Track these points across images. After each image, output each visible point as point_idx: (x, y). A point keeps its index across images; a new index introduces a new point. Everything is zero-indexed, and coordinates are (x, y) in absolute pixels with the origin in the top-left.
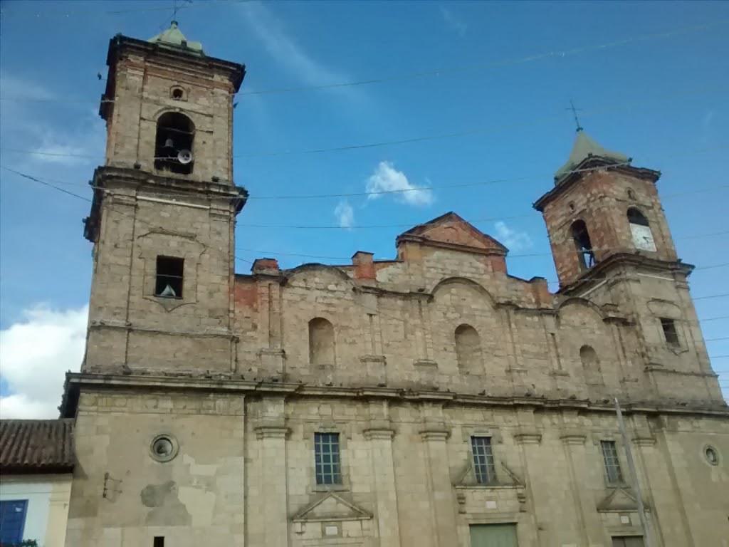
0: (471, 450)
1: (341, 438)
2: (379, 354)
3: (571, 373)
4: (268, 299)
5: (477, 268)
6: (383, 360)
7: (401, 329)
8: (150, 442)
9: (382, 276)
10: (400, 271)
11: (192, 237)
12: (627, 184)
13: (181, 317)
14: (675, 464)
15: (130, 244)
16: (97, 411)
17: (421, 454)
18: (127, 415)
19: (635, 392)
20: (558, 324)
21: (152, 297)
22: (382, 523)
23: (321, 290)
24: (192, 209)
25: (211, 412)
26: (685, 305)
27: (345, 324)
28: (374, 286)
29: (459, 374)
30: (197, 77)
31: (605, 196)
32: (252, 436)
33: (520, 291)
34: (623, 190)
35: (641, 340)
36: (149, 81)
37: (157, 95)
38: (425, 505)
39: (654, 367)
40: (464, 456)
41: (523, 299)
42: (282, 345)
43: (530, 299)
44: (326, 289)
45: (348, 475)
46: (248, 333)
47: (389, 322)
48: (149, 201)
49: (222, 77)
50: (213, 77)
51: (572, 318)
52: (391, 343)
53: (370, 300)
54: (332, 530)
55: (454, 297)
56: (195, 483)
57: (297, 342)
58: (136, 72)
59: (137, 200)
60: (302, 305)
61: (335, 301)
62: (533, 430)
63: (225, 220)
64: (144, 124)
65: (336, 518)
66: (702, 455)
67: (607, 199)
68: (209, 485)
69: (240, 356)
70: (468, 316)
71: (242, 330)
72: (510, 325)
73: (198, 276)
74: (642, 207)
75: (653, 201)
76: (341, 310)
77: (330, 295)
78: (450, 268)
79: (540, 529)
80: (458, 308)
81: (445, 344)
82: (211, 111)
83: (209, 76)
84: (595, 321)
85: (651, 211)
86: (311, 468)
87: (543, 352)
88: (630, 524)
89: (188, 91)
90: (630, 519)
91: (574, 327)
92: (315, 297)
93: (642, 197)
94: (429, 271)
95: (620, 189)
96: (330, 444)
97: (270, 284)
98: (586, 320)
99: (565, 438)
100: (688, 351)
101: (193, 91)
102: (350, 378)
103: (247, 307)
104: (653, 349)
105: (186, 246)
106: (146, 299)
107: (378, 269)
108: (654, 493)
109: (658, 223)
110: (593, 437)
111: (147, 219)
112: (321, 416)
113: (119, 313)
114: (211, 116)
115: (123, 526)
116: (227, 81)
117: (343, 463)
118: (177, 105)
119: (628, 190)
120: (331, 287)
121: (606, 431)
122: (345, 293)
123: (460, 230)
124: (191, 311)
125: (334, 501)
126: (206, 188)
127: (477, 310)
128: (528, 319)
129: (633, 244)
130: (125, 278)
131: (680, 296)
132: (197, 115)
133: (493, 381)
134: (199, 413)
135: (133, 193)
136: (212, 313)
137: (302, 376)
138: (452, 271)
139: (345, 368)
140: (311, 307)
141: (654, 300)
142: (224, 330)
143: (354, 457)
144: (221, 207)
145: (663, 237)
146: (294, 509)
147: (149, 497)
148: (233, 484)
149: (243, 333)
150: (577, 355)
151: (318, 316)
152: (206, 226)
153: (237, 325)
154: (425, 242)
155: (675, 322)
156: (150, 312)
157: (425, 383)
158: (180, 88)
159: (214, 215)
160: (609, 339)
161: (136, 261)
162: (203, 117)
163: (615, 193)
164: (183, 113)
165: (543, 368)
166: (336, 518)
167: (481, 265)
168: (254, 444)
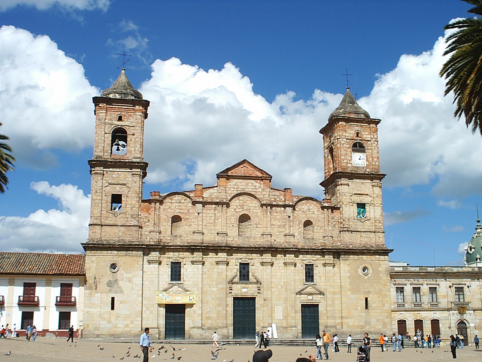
0: (239, 268)
3: (296, 234)
4: (154, 209)
5: (255, 186)
7: (213, 218)
8: (109, 265)
9: (206, 194)
10: (215, 191)
11: (124, 185)
23: (178, 203)
27: (187, 217)
28: (201, 200)
29: (238, 236)
31: (340, 138)
33: (277, 195)
34: (354, 132)
35: (342, 215)
36: (108, 114)
37: (111, 120)
39: (344, 229)
40: (235, 271)
41: (278, 199)
43: (282, 199)
46: (146, 223)
47: (208, 215)
51: (303, 207)
52: (207, 224)
53: (199, 206)
55: (240, 201)
56: (125, 280)
57: (166, 226)
59: (103, 171)
60: (169, 210)
61: (184, 208)
62: (269, 260)
63: (138, 176)
64: (106, 136)
66: (360, 271)
70: (246, 210)
71: (144, 222)
73: (127, 201)
74: (363, 141)
75: (372, 136)
77: (182, 204)
78: (241, 187)
80: (242, 206)
81: (233, 224)
82: (134, 124)
84: (316, 208)
85: (369, 143)
89: (125, 116)
90: (313, 297)
93: (366, 135)
94: (230, 190)
95: (352, 132)
101: (127, 115)
103: (146, 212)
104: (347, 220)
111: (108, 179)
115: (101, 293)
118: (120, 123)
123: (249, 167)
124: (124, 216)
125: (177, 287)
127: (252, 206)
128: (279, 209)
129: (352, 164)
130: (100, 205)
132: (128, 127)
133: (254, 239)
136: (132, 216)
137: (167, 240)
138: (242, 189)
139: (185, 236)
140: (173, 211)
141: (355, 194)
142: (136, 223)
147: (110, 284)
148: (138, 280)
149: (144, 223)
153: (142, 220)
154: (229, 178)
155: (366, 205)
156: (110, 217)
158: (121, 115)
159: (133, 174)
160: (322, 216)
161: (104, 197)
163: (347, 135)
164: (122, 127)
165: (281, 232)
167: (258, 184)
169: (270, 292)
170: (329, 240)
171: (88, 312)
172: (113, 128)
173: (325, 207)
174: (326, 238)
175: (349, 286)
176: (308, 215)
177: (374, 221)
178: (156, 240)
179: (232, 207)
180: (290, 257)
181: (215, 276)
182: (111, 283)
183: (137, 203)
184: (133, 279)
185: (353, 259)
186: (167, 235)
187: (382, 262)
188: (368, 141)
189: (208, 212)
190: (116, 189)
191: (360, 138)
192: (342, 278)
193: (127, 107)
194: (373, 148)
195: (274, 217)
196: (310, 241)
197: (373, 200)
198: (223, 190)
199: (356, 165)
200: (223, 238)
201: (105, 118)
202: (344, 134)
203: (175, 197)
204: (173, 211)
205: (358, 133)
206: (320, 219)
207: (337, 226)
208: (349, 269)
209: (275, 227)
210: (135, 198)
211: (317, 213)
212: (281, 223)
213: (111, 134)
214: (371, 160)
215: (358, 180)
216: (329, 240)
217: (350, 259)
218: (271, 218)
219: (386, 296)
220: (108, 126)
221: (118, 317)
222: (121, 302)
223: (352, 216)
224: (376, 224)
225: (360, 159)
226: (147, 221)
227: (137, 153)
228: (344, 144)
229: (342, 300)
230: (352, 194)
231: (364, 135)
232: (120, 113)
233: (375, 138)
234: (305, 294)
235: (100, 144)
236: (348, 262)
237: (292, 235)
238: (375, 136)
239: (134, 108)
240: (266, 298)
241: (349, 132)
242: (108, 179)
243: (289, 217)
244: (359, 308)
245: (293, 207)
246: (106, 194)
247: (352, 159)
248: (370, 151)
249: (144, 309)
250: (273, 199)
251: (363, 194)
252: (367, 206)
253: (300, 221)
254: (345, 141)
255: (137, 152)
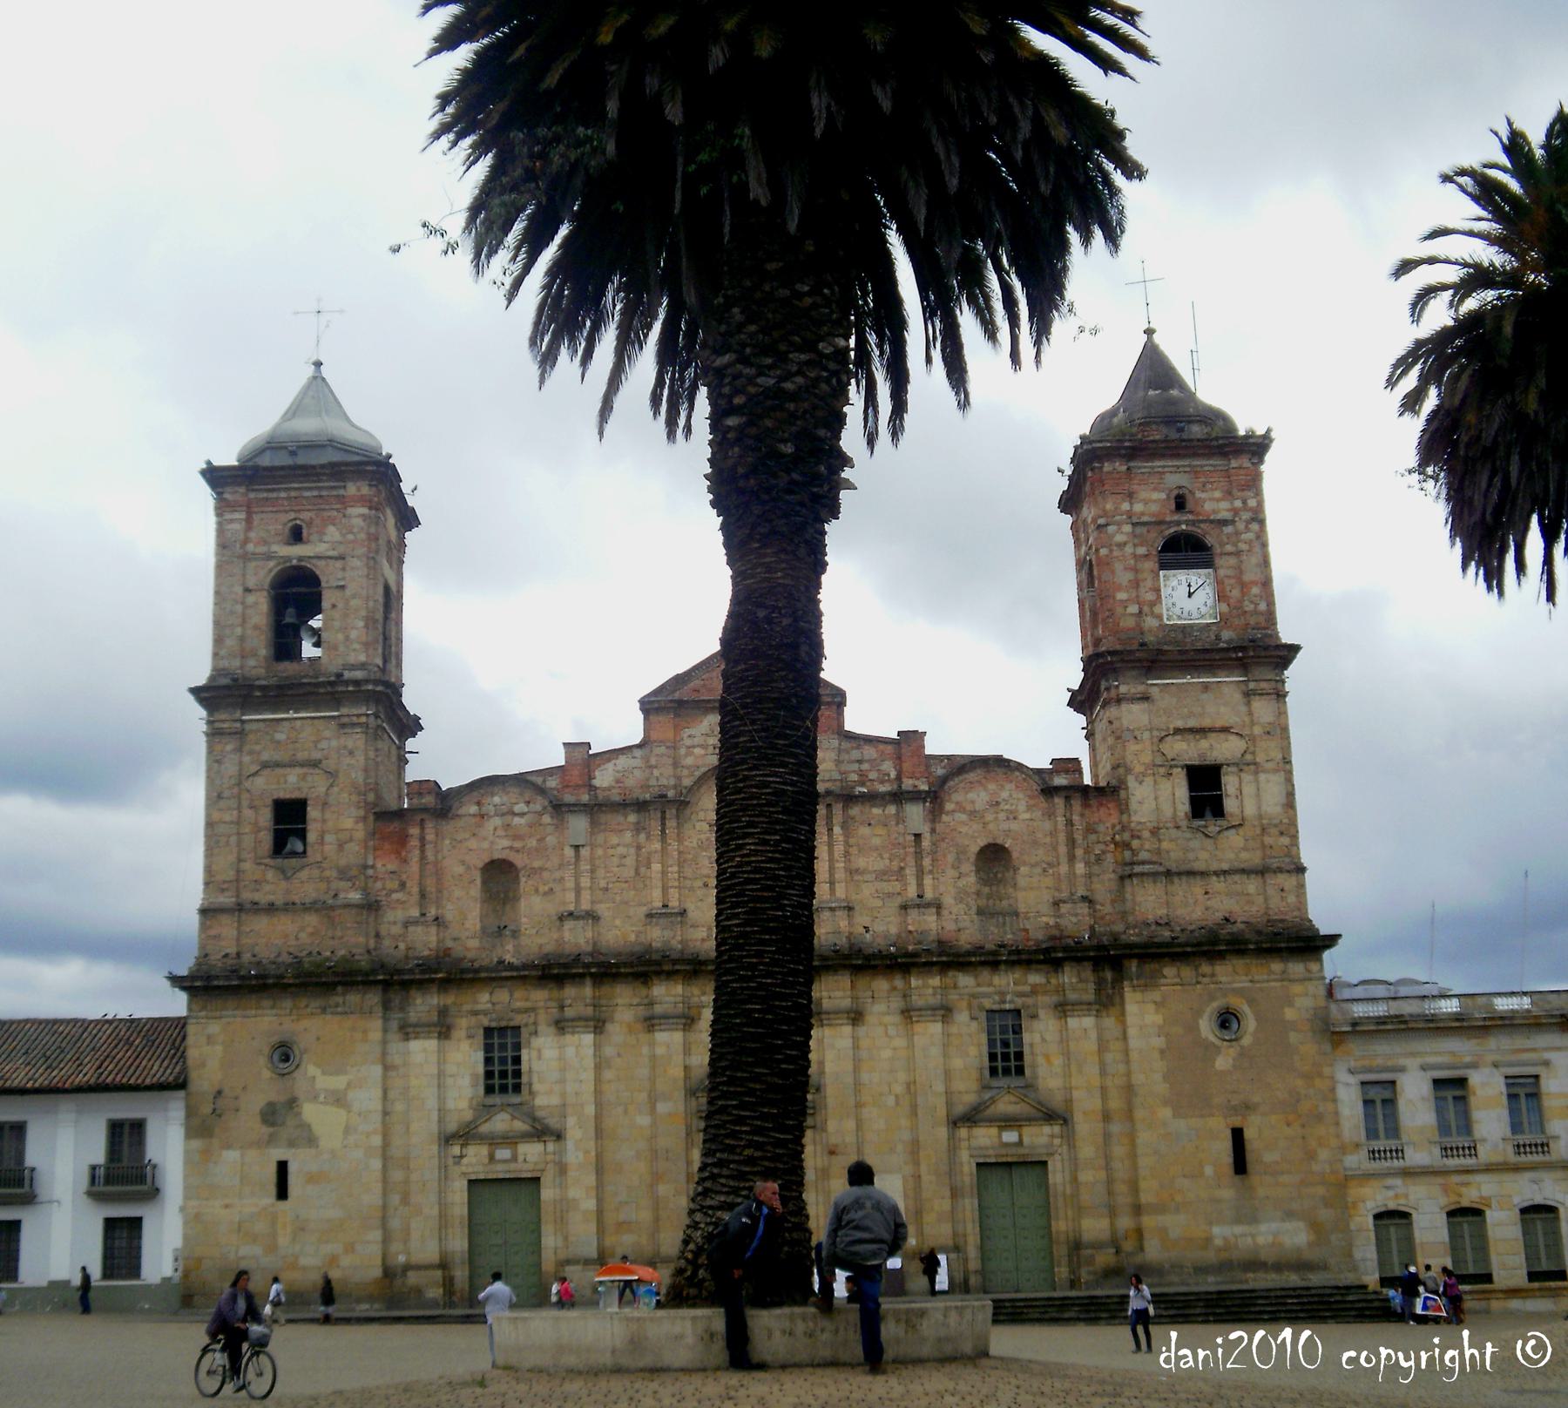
1: (523, 1030)
2: (585, 905)
3: (948, 900)
6: (592, 916)
9: (604, 778)
10: (638, 762)
11: (315, 764)
12: (1175, 480)
13: (306, 885)
14: (1135, 1042)
15: (235, 790)
16: (207, 1018)
17: (645, 1050)
18: (239, 1019)
19: (1076, 923)
20: (935, 814)
21: (267, 861)
22: (570, 1144)
24: (316, 721)
25: (339, 1009)
26: (1257, 730)
27: (537, 864)
28: (585, 798)
30: (321, 496)
31: (1107, 525)
32: (394, 1036)
33: (868, 761)
34: (1163, 496)
35: (1125, 817)
36: (255, 523)
37: (265, 542)
38: (644, 1120)
39: (1138, 869)
41: (873, 775)
42: (437, 909)
44: (515, 814)
45: (530, 1084)
46: (395, 896)
47: (611, 852)
48: (258, 720)
49: (358, 484)
50: (345, 487)
51: (971, 796)
53: (578, 825)
54: (503, 1153)
56: (322, 1098)
58: (237, 516)
59: (243, 722)
60: (473, 844)
64: (251, 599)
65: (510, 1140)
66: (1207, 1027)
67: (1111, 529)
68: (339, 1099)
69: (383, 931)
72: (830, 830)
74: (1202, 525)
75: (1238, 504)
76: (533, 843)
77: (517, 820)
79: (832, 1153)
82: (341, 549)
83: (340, 487)
84: (1021, 796)
85: (1229, 529)
86: (474, 1076)
87: (896, 868)
88: (1020, 1143)
89: (310, 524)
91: (973, 814)
92: (492, 828)
93: (1212, 502)
94: (687, 755)
95: (1155, 496)
96: (509, 1040)
97: (422, 820)
98: (1005, 794)
99: (908, 1014)
100: (1240, 825)
101: (317, 521)
102: (541, 946)
103: (393, 856)
104: (1146, 834)
105: (309, 778)
106: (260, 864)
107: (599, 765)
108: (1076, 1094)
109: (1238, 553)
110: (970, 1007)
111: (257, 748)
112: (493, 1004)
113: (227, 889)
114: (342, 558)
116: (365, 490)
117: (524, 1067)
119: (1175, 492)
120: (517, 808)
121: (1002, 994)
122: (540, 814)
124: (316, 873)
126: (329, 689)
128: (876, 811)
129: (1160, 617)
130: (233, 839)
131: (1250, 714)
132: (322, 563)
134: (324, 1010)
135: (237, 715)
136: (343, 874)
137: (467, 949)
139: (534, 931)
140: (486, 845)
141: (1178, 731)
143: (539, 1058)
144: (355, 711)
145: (1244, 586)
146: (452, 1127)
147: (271, 1115)
148: (367, 1098)
150: (968, 867)
151: (496, 856)
152: (334, 743)
153: (379, 885)
155: (1224, 769)
157: (659, 945)
160: (1048, 825)
162: (331, 562)
163: (1138, 507)
164: (303, 564)
165: (890, 895)
166: (510, 1140)
168: (396, 1046)
169: (850, 1124)
170: (1076, 915)
171: (197, 1216)
172: (270, 571)
173: (1057, 789)
174: (1064, 908)
175: (1162, 1088)
176: (991, 826)
177: (1258, 831)
178: (426, 953)
179: (701, 815)
180: (926, 986)
181: (644, 1072)
182: (274, 1113)
183: (361, 826)
184: (351, 1095)
185: (1177, 980)
186: (467, 934)
187: (1297, 989)
188: (1224, 522)
189: (614, 840)
190: (286, 782)
191: (1191, 517)
192: (1134, 1056)
193: (315, 493)
194: (1242, 546)
195: (861, 842)
196: (1004, 923)
197: (1252, 749)
198: (662, 755)
199: (1179, 618)
200: (668, 934)
201: (242, 537)
202: (1125, 506)
203: (493, 795)
204: (486, 845)
205: (1180, 503)
206: (1039, 835)
207: (1109, 858)
208: (1159, 1019)
209: (868, 877)
210: (353, 809)
211: (1027, 816)
212: (887, 862)
213: (265, 593)
214: (1236, 593)
215: (1188, 679)
216: (1076, 915)
217: (1163, 981)
218: (847, 844)
219: (1319, 1118)
220: (253, 564)
221: (303, 1229)
222: (312, 1179)
223: (1168, 811)
224: (1268, 840)
225: (1190, 595)
226: (396, 885)
227: (354, 650)
228: (1125, 544)
229: (1139, 1141)
230: (1163, 734)
231: (1204, 500)
232: (293, 515)
233: (1251, 509)
234: (991, 1121)
235: (227, 632)
236: (1156, 995)
237: (928, 905)
238: (1252, 503)
239: (342, 492)
240: (836, 1146)
241: (1143, 495)
242: (257, 748)
243: (918, 836)
244: (1209, 1170)
245: (934, 798)
246: (252, 800)
247: (1159, 597)
248: (1232, 561)
249: (395, 1199)
250: (854, 777)
251: (1212, 730)
252: (1227, 774)
253: (961, 853)
254: (1127, 534)
255: (356, 646)
